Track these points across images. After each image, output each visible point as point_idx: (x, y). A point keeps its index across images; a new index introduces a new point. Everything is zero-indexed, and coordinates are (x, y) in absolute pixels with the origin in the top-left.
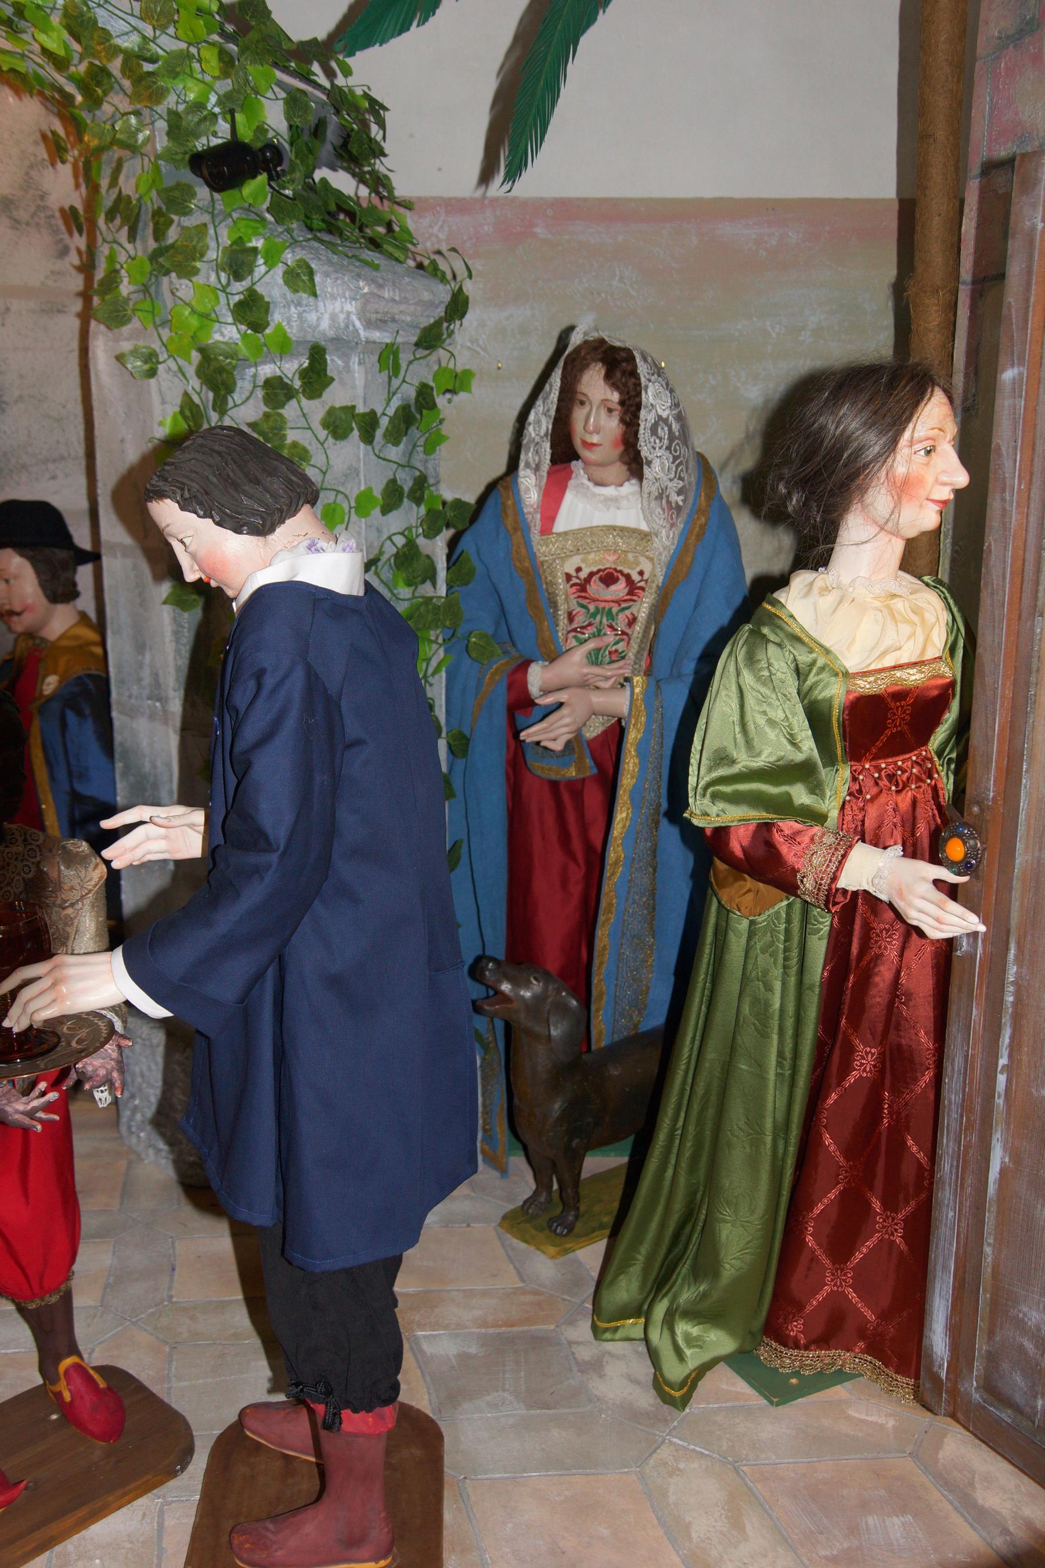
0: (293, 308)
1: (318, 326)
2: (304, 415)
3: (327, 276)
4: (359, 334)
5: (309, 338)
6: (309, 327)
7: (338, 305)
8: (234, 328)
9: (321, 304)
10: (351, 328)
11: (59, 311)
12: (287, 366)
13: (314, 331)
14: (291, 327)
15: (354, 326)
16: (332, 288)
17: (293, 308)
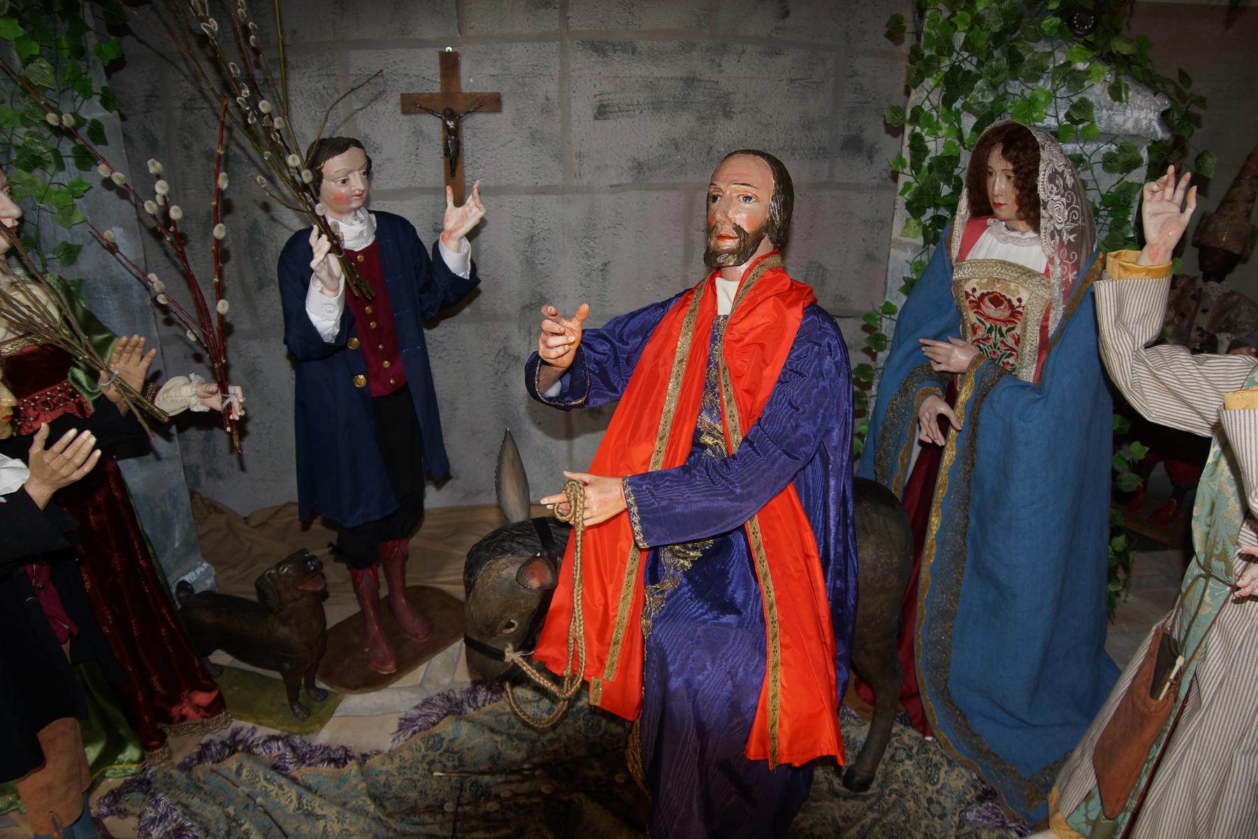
0: (1104, 111)
1: (1123, 125)
2: (1095, 180)
3: (1139, 93)
4: (1157, 135)
5: (1114, 132)
6: (1117, 125)
7: (1143, 114)
8: (1053, 119)
9: (1128, 112)
10: (1152, 130)
11: (777, 54)
12: (1086, 147)
13: (1119, 128)
14: (1100, 123)
15: (1154, 129)
16: (1141, 102)
17: (1104, 111)
